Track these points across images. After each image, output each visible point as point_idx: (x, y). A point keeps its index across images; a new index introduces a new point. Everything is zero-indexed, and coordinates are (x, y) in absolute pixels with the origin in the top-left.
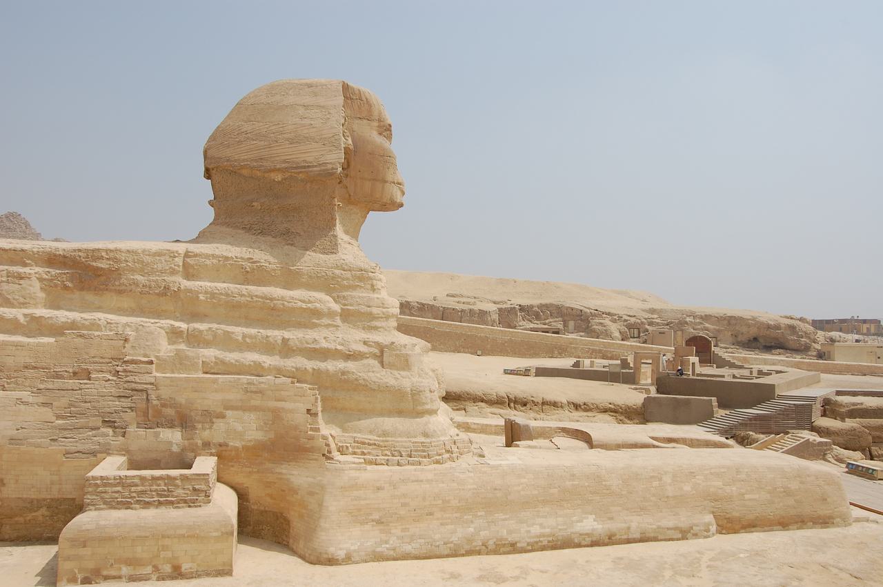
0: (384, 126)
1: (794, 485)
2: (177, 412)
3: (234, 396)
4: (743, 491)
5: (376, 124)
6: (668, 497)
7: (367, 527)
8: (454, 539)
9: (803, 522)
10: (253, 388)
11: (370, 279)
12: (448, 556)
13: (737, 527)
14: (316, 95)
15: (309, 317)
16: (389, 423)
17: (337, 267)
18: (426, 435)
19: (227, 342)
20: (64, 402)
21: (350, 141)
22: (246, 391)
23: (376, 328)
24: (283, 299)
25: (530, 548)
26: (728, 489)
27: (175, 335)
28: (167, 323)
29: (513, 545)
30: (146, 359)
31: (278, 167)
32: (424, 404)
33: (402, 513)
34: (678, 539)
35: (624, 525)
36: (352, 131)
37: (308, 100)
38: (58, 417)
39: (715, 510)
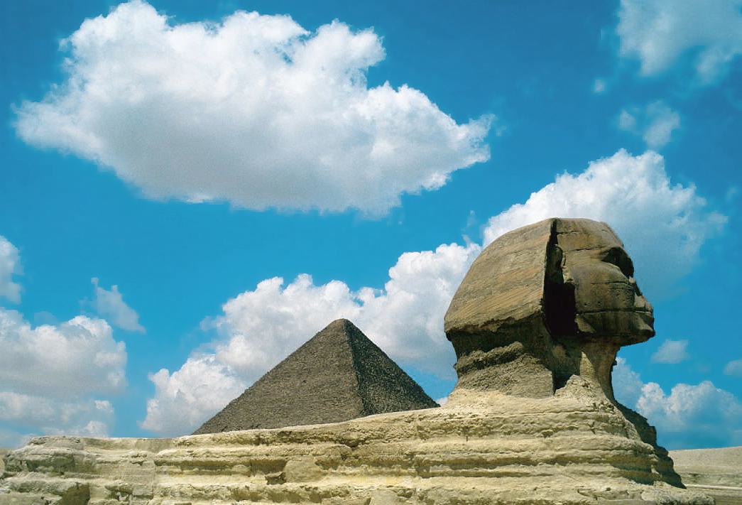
0: (605, 252)
5: (597, 251)
11: (585, 418)
14: (526, 239)
24: (496, 450)
31: (491, 318)
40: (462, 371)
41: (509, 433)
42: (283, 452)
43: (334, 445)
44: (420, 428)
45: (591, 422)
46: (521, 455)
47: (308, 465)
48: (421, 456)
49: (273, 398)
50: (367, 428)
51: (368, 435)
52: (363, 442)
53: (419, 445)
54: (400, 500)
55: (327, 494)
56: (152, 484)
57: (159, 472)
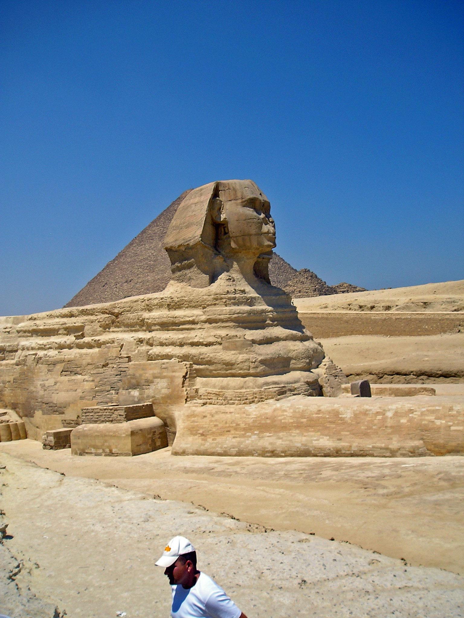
2: (137, 381)
4: (450, 424)
5: (239, 201)
6: (386, 427)
7: (196, 437)
10: (164, 366)
11: (221, 299)
13: (443, 451)
14: (201, 195)
17: (206, 295)
20: (98, 379)
22: (161, 368)
24: (179, 317)
25: (283, 454)
26: (438, 422)
29: (272, 452)
30: (126, 356)
33: (214, 430)
35: (347, 444)
37: (196, 200)
39: (425, 437)
40: (174, 271)
41: (187, 307)
42: (82, 321)
43: (108, 316)
44: (148, 305)
45: (224, 300)
46: (191, 319)
47: (95, 327)
48: (147, 320)
49: (141, 258)
50: (122, 305)
51: (122, 310)
52: (121, 314)
53: (146, 315)
54: (138, 344)
55: (104, 343)
56: (16, 343)
57: (20, 337)
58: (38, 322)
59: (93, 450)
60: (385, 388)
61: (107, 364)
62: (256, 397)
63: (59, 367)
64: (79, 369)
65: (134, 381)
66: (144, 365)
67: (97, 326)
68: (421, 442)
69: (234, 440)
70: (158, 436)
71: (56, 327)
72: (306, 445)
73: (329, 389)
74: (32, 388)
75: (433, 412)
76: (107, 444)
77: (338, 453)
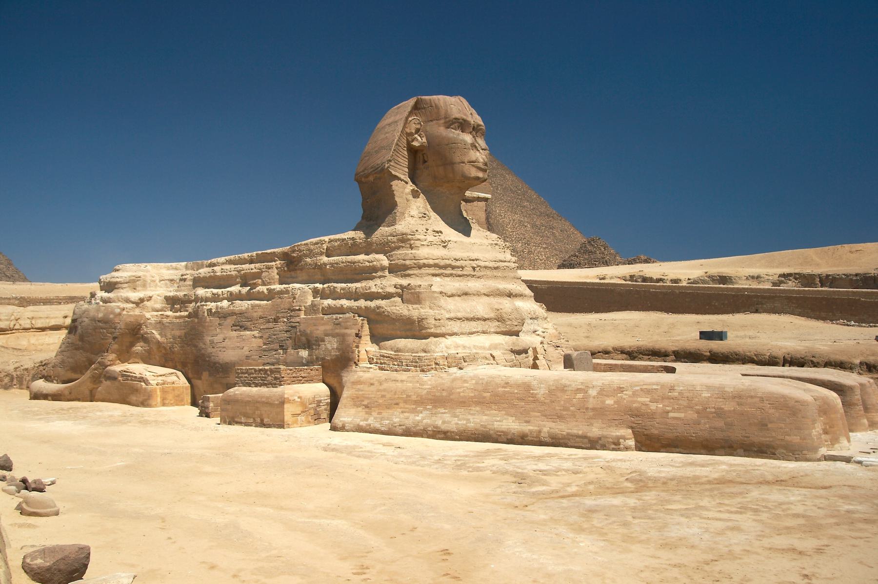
1: (728, 406)
3: (328, 327)
5: (442, 121)
6: (587, 409)
7: (360, 409)
8: (407, 422)
9: (731, 447)
10: (337, 322)
11: (409, 240)
12: (402, 435)
15: (369, 272)
16: (401, 343)
17: (391, 235)
18: (425, 352)
19: (334, 295)
21: (424, 140)
23: (409, 275)
24: (359, 262)
26: (653, 406)
27: (316, 292)
28: (312, 286)
32: (427, 328)
33: (381, 401)
34: (586, 449)
35: (536, 428)
36: (426, 132)
38: (265, 344)
50: (302, 248)
53: (325, 259)
58: (215, 268)
59: (243, 420)
60: (616, 365)
61: (278, 318)
62: (436, 364)
63: (230, 321)
64: (249, 323)
65: (304, 339)
66: (317, 319)
67: (274, 273)
68: (630, 431)
69: (402, 416)
70: (323, 408)
71: (233, 273)
72: (485, 427)
73: (544, 362)
74: (201, 345)
75: (648, 392)
76: (258, 412)
77: (522, 440)
